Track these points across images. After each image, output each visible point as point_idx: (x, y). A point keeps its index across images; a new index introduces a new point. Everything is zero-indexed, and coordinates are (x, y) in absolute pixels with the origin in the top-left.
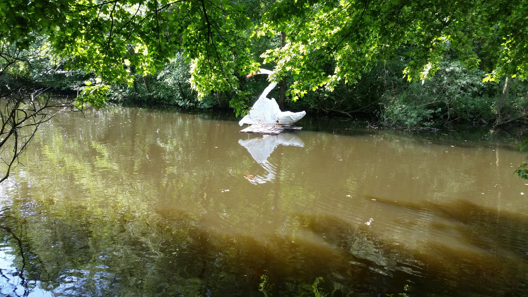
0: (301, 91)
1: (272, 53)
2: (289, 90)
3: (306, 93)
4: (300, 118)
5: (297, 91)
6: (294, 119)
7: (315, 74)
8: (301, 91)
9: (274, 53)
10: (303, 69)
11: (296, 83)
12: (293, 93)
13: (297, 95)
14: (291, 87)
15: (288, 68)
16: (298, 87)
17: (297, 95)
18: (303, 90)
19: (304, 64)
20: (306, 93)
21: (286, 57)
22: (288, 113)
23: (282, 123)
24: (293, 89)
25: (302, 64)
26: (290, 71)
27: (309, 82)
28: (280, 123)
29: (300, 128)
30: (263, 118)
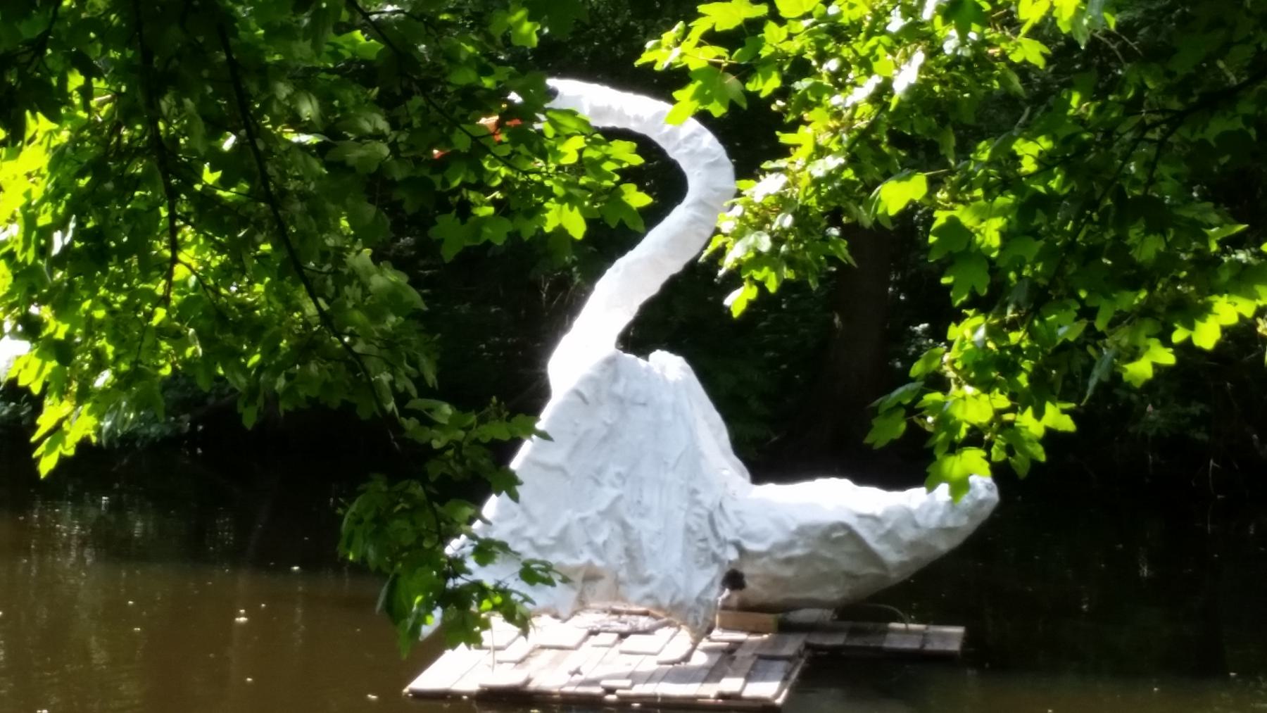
0: (1019, 401)
1: (754, 26)
2: (901, 394)
3: (1067, 424)
4: (944, 546)
5: (973, 406)
6: (892, 556)
7: (1147, 248)
8: (1019, 401)
9: (772, 33)
10: (1047, 202)
11: (970, 332)
12: (946, 422)
13: (976, 438)
14: (917, 369)
15: (896, 195)
16: (988, 370)
17: (976, 438)
18: (1034, 399)
19: (1046, 163)
20: (1067, 424)
21: (884, 65)
22: (833, 499)
23: (779, 596)
24: (938, 382)
25: (1028, 166)
26: (912, 221)
27: (1088, 313)
28: (755, 589)
29: (951, 637)
30: (615, 556)
